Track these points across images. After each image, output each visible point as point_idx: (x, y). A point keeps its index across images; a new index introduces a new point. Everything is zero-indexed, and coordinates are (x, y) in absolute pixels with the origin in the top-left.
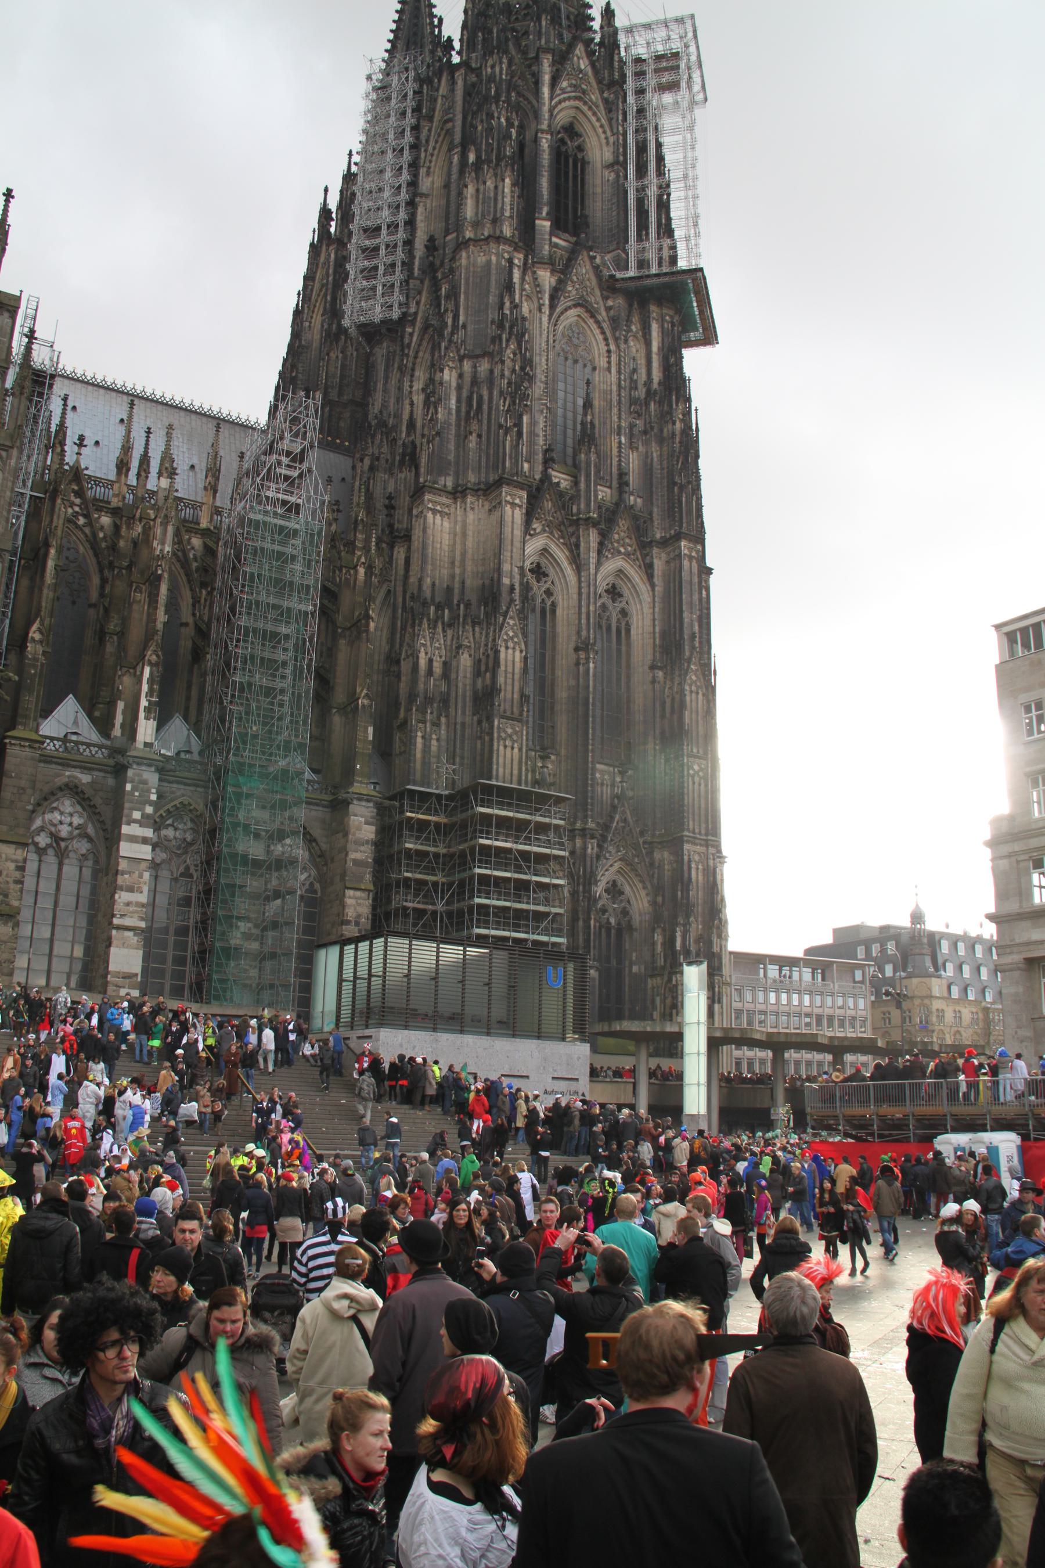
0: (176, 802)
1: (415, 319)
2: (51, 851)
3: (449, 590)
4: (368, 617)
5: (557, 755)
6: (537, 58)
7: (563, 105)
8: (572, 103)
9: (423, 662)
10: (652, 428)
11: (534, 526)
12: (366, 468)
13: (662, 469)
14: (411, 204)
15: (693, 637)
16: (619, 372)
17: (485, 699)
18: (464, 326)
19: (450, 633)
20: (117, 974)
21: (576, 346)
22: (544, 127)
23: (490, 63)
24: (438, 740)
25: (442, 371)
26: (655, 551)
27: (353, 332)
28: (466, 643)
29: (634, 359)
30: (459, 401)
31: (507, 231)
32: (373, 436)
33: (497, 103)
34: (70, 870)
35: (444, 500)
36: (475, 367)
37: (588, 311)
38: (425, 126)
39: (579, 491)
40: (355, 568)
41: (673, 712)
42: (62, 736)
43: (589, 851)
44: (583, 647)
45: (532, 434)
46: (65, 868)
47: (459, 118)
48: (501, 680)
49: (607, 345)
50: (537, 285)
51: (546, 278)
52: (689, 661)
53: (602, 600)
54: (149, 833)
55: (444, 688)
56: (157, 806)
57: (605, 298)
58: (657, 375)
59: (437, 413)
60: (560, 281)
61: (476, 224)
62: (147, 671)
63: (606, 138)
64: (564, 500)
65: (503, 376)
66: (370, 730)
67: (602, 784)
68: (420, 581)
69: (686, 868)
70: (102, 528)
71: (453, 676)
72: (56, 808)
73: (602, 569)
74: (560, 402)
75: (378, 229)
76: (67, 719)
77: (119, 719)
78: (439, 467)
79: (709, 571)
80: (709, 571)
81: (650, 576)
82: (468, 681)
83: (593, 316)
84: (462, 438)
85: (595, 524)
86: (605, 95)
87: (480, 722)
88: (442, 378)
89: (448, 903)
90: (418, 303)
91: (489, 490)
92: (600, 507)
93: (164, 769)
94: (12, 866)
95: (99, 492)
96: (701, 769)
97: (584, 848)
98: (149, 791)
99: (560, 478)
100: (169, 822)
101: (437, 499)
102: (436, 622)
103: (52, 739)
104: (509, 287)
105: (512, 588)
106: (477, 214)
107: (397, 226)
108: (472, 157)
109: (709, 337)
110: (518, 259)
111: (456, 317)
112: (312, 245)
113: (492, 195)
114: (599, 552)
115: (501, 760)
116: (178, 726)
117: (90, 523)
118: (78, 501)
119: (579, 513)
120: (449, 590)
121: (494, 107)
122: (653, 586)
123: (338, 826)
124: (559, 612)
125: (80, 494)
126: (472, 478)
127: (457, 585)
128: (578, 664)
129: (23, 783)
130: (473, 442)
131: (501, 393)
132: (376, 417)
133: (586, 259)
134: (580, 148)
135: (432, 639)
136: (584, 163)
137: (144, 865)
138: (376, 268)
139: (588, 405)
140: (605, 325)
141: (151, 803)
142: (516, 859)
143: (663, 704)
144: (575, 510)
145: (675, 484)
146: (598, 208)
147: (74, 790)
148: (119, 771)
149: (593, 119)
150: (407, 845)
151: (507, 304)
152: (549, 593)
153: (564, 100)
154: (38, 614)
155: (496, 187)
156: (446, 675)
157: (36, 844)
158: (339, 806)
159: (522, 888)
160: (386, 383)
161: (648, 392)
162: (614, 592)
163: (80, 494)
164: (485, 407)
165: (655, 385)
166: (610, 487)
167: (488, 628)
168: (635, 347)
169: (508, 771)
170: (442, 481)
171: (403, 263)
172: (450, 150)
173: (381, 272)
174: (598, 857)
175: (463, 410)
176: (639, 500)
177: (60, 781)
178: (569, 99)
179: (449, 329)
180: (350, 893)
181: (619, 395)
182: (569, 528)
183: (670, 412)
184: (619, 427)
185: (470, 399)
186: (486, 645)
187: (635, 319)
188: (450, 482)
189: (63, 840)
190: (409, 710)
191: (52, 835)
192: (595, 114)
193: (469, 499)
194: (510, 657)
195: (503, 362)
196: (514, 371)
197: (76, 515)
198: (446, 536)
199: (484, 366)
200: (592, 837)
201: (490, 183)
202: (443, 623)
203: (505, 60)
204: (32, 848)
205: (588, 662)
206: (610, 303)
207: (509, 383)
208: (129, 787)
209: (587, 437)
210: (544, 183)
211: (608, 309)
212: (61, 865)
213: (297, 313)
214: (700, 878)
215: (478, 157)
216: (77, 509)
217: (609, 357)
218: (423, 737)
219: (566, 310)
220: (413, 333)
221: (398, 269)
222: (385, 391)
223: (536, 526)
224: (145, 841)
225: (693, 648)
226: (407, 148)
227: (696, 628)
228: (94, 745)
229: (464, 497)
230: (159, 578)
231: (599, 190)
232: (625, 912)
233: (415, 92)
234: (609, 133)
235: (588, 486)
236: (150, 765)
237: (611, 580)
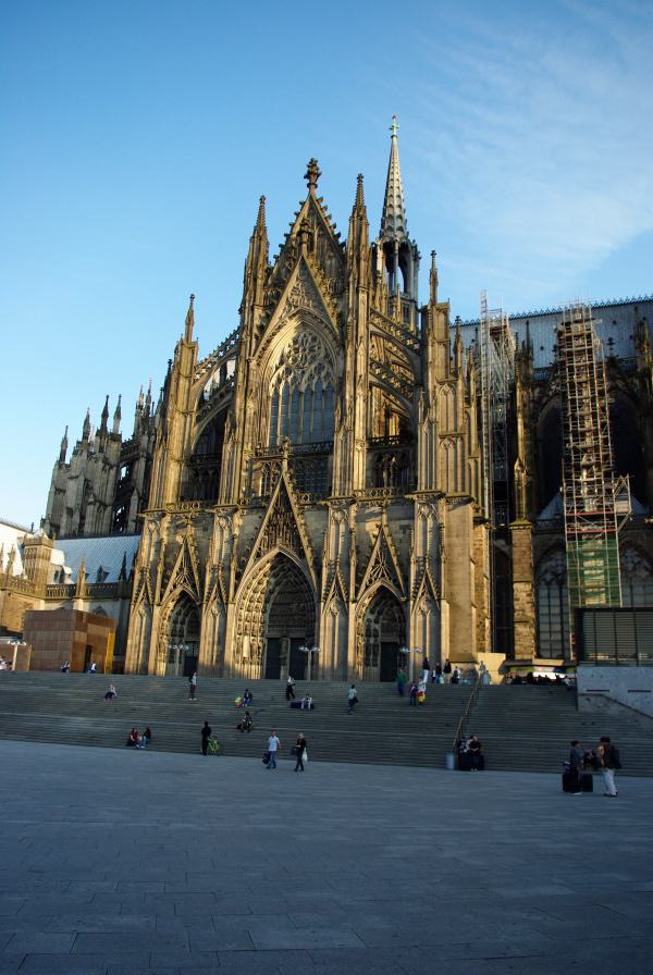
2: (554, 582)
94: (524, 594)
129: (523, 549)
154: (517, 456)
157: (545, 580)
177: (551, 543)
204: (543, 583)
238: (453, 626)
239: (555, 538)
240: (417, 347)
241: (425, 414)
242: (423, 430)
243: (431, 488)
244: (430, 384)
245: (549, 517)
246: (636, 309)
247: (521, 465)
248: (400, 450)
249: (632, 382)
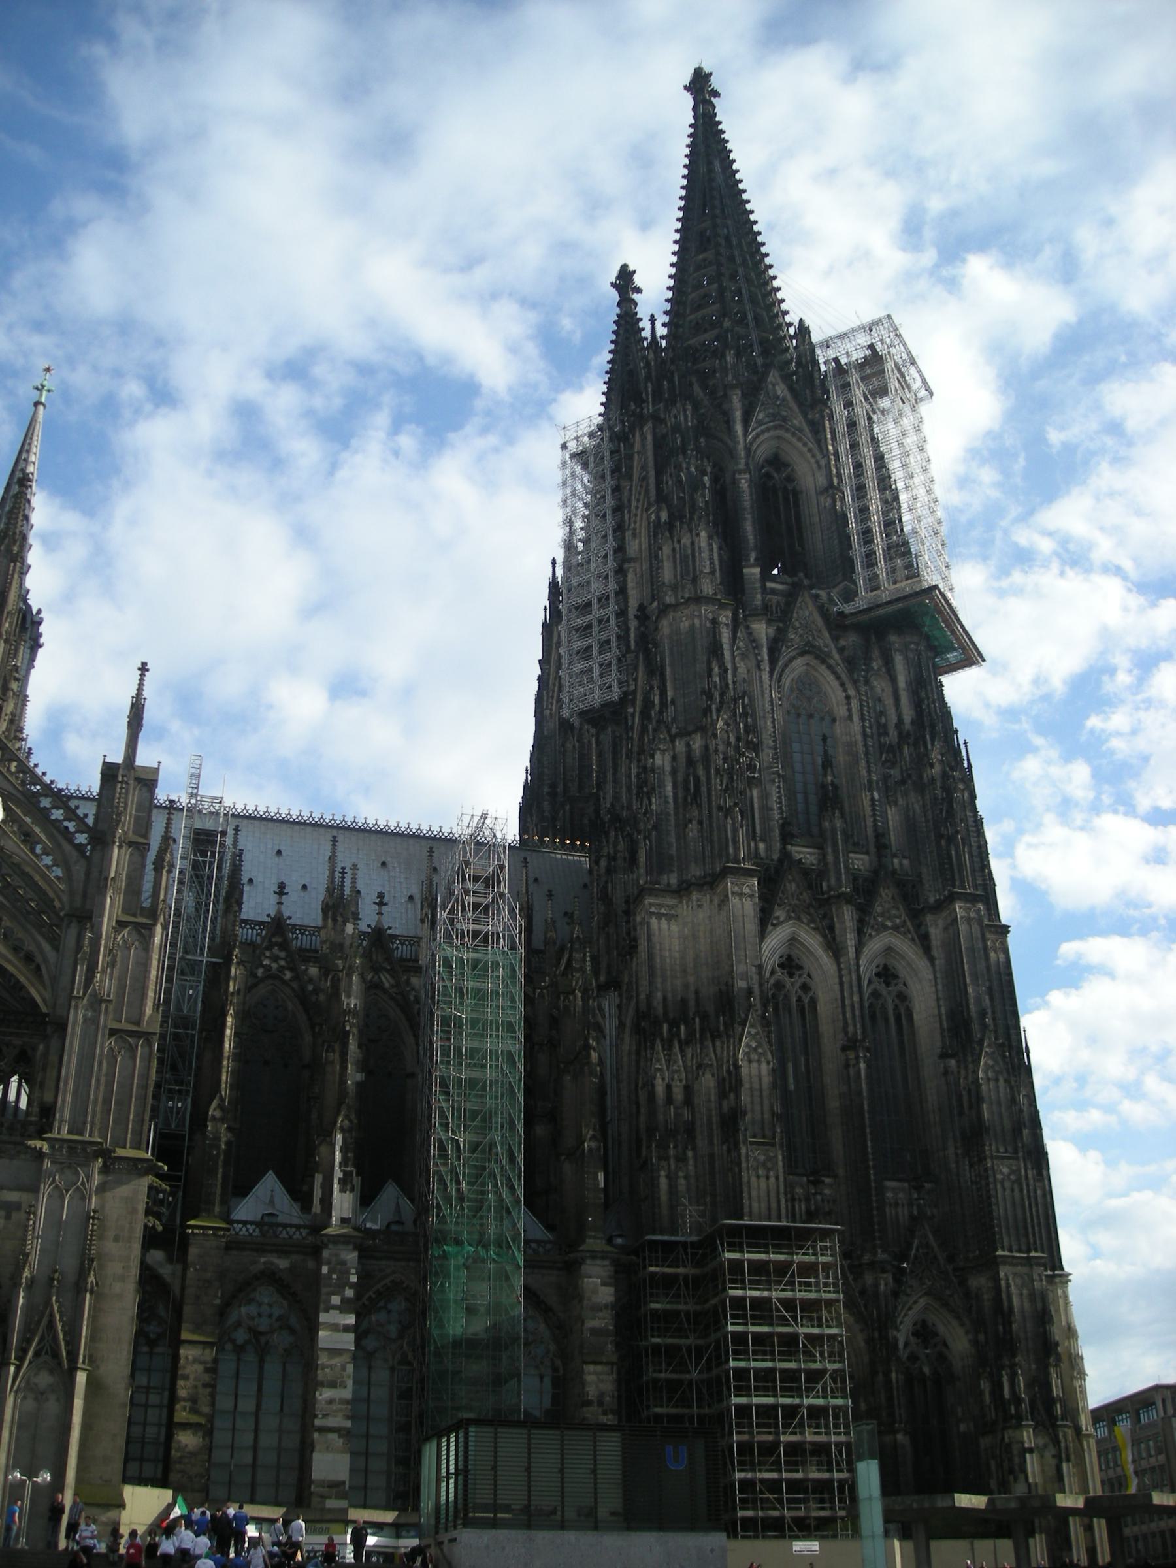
0: (387, 1281)
1: (635, 699)
3: (684, 1001)
4: (587, 1047)
5: (835, 1176)
6: (725, 395)
7: (762, 438)
8: (772, 433)
9: (660, 1089)
10: (909, 776)
11: (777, 914)
12: (603, 870)
13: (927, 821)
14: (620, 571)
15: (983, 1014)
16: (863, 719)
17: (730, 1123)
18: (673, 702)
19: (689, 1051)
20: (322, 1484)
21: (809, 699)
22: (742, 466)
23: (674, 411)
24: (686, 1177)
25: (653, 756)
26: (929, 918)
27: (575, 721)
28: (706, 1061)
29: (880, 700)
30: (675, 786)
31: (707, 588)
32: (607, 834)
33: (684, 453)
34: (273, 1368)
35: (668, 901)
36: (688, 745)
37: (817, 657)
38: (625, 484)
39: (826, 864)
40: (573, 992)
41: (970, 1107)
42: (258, 1218)
43: (882, 1287)
44: (850, 1045)
45: (766, 808)
46: (267, 1366)
47: (652, 473)
48: (745, 1098)
49: (845, 690)
50: (752, 640)
51: (762, 629)
52: (981, 1042)
53: (872, 987)
54: (351, 1319)
55: (687, 1115)
56: (359, 1288)
57: (835, 639)
58: (908, 714)
59: (650, 804)
60: (779, 630)
61: (674, 588)
62: (339, 1137)
63: (817, 462)
64: (812, 878)
65: (716, 751)
66: (601, 1176)
67: (897, 1205)
68: (649, 997)
69: (1004, 1296)
70: (311, 980)
71: (696, 1101)
72: (253, 1300)
73: (866, 951)
74: (798, 767)
75: (589, 604)
76: (266, 1197)
77: (318, 1193)
78: (660, 863)
79: (1005, 930)
80: (1005, 930)
82: (713, 1105)
83: (823, 662)
84: (682, 825)
85: (848, 899)
86: (810, 416)
87: (729, 1151)
88: (653, 763)
89: (709, 1368)
90: (635, 680)
91: (711, 882)
92: (855, 879)
93: (366, 1244)
94: (199, 1368)
95: (305, 941)
96: (1012, 1172)
97: (877, 1285)
98: (348, 1273)
99: (804, 853)
100: (381, 1304)
101: (661, 901)
102: (670, 1042)
103: (245, 1223)
104: (715, 650)
105: (749, 992)
106: (675, 576)
107: (607, 598)
108: (664, 516)
109: (970, 656)
110: (725, 617)
111: (663, 693)
112: (544, 625)
113: (689, 552)
114: (860, 932)
115: (754, 1193)
116: (390, 1193)
117: (296, 977)
118: (283, 954)
119: (830, 888)
120: (684, 1001)
121: (681, 458)
122: (932, 960)
123: (571, 1293)
124: (821, 1008)
125: (284, 946)
126: (696, 871)
127: (691, 997)
128: (847, 1066)
130: (693, 831)
131: (717, 771)
132: (609, 812)
133: (808, 599)
134: (790, 479)
135: (668, 1061)
136: (796, 494)
137: (346, 1358)
138: (590, 647)
139: (827, 763)
140: (839, 669)
141: (352, 1286)
142: (778, 1310)
143: (961, 1096)
144: (824, 885)
145: (941, 836)
146: (818, 540)
147: (270, 1277)
148: (316, 1251)
149: (800, 445)
150: (654, 1306)
151: (716, 670)
152: (805, 988)
153: (763, 432)
155: (693, 543)
156: (688, 1101)
157: (233, 1341)
158: (572, 1268)
159: (790, 1344)
160: (614, 774)
161: (900, 734)
162: (886, 974)
163: (284, 946)
164: (704, 789)
165: (907, 726)
166: (867, 853)
167: (728, 1042)
168: (880, 685)
169: (764, 1205)
170: (664, 879)
171: (619, 637)
172: (647, 510)
173: (595, 651)
174: (896, 1294)
175: (680, 795)
176: (906, 862)
178: (768, 430)
179: (657, 708)
180: (591, 1368)
181: (865, 745)
182: (819, 910)
183: (927, 754)
184: (870, 781)
185: (686, 781)
186: (728, 1061)
187: (876, 653)
188: (673, 880)
189: (261, 1334)
190: (649, 1147)
191: (250, 1329)
192: (800, 439)
193: (695, 896)
194: (754, 1072)
195: (715, 736)
196: (729, 744)
197: (281, 969)
198: (676, 942)
199: (697, 743)
200: (884, 1271)
201: (686, 540)
202: (680, 1042)
203: (689, 407)
204: (229, 1346)
205: (858, 1063)
206: (842, 642)
207: (725, 759)
208: (325, 1269)
209: (829, 799)
210: (749, 528)
211: (841, 650)
212: (261, 1362)
213: (539, 700)
214: (1027, 1305)
215: (671, 515)
216: (282, 963)
217: (849, 704)
218: (667, 1177)
219: (791, 660)
220: (634, 711)
221: (614, 645)
222: (615, 781)
223: (780, 913)
224: (347, 1329)
225: (984, 1026)
226: (609, 512)
227: (987, 1001)
228: (291, 1226)
229: (690, 893)
230: (347, 1034)
231: (816, 519)
232: (942, 1358)
233: (612, 453)
234: (819, 456)
235: (837, 858)
236: (347, 1243)
237: (880, 961)
238: (86, 1426)
239: (263, 1260)
240: (82, 839)
241: (89, 980)
242: (77, 1018)
243: (81, 1134)
244: (106, 920)
245: (250, 1218)
246: (431, 851)
247: (220, 1107)
248: (17, 1042)
249: (408, 982)
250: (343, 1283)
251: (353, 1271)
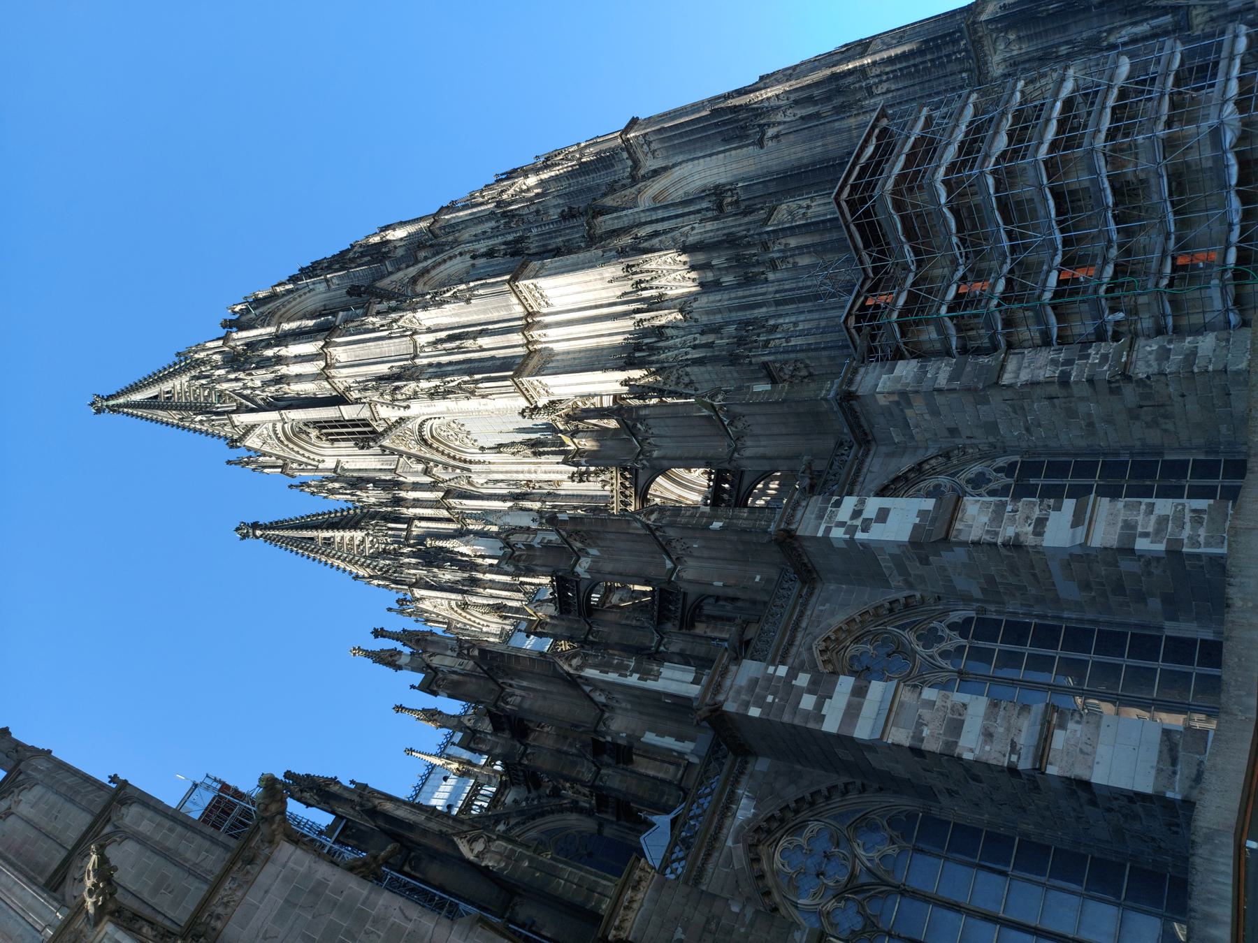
26: (642, 172)
81: (665, 169)
87: (773, 265)
98: (770, 678)
122: (674, 165)
141: (793, 674)
208: (754, 712)
250: (787, 689)
251: (771, 669)
